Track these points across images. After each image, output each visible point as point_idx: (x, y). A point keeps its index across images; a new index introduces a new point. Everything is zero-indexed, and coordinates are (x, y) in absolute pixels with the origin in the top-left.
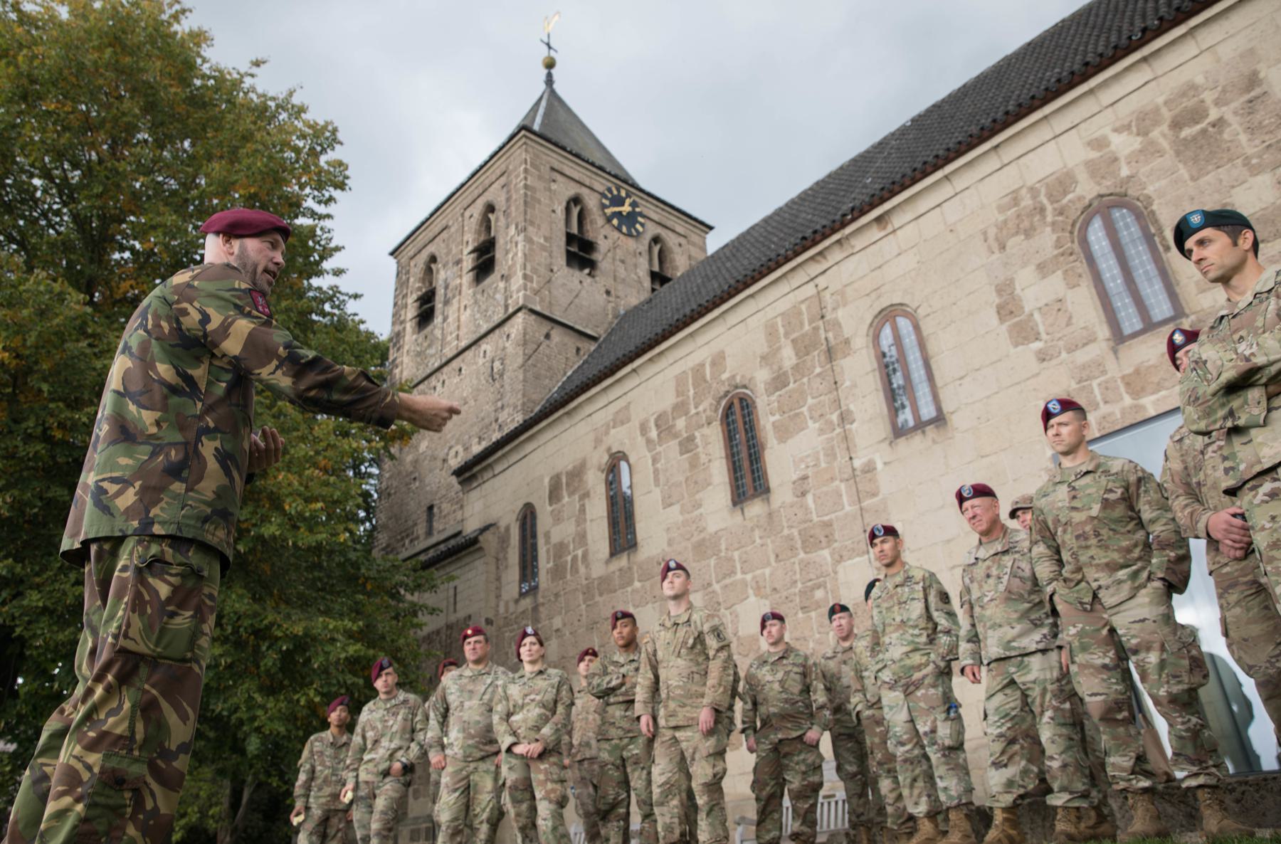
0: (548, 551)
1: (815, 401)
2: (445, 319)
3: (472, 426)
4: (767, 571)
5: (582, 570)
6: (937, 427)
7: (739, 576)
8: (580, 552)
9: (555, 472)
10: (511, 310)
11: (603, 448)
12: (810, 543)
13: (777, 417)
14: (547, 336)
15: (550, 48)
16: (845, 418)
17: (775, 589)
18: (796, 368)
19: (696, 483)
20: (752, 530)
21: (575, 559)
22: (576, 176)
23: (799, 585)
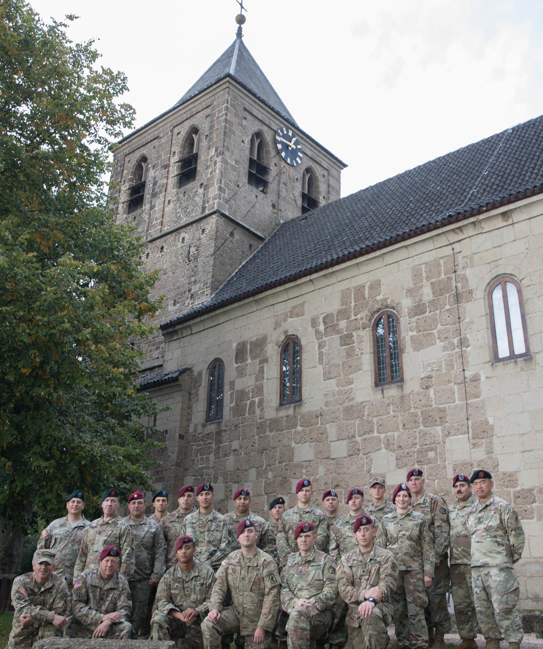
0: (232, 395)
1: (443, 327)
2: (152, 207)
3: (169, 291)
4: (396, 434)
5: (258, 412)
6: (525, 360)
7: (375, 434)
8: (257, 400)
9: (242, 340)
10: (207, 212)
11: (281, 330)
12: (428, 420)
13: (415, 333)
14: (232, 234)
15: (242, 7)
16: (463, 343)
17: (400, 447)
18: (432, 302)
19: (350, 367)
20: (388, 405)
21: (252, 403)
22: (260, 116)
23: (418, 447)
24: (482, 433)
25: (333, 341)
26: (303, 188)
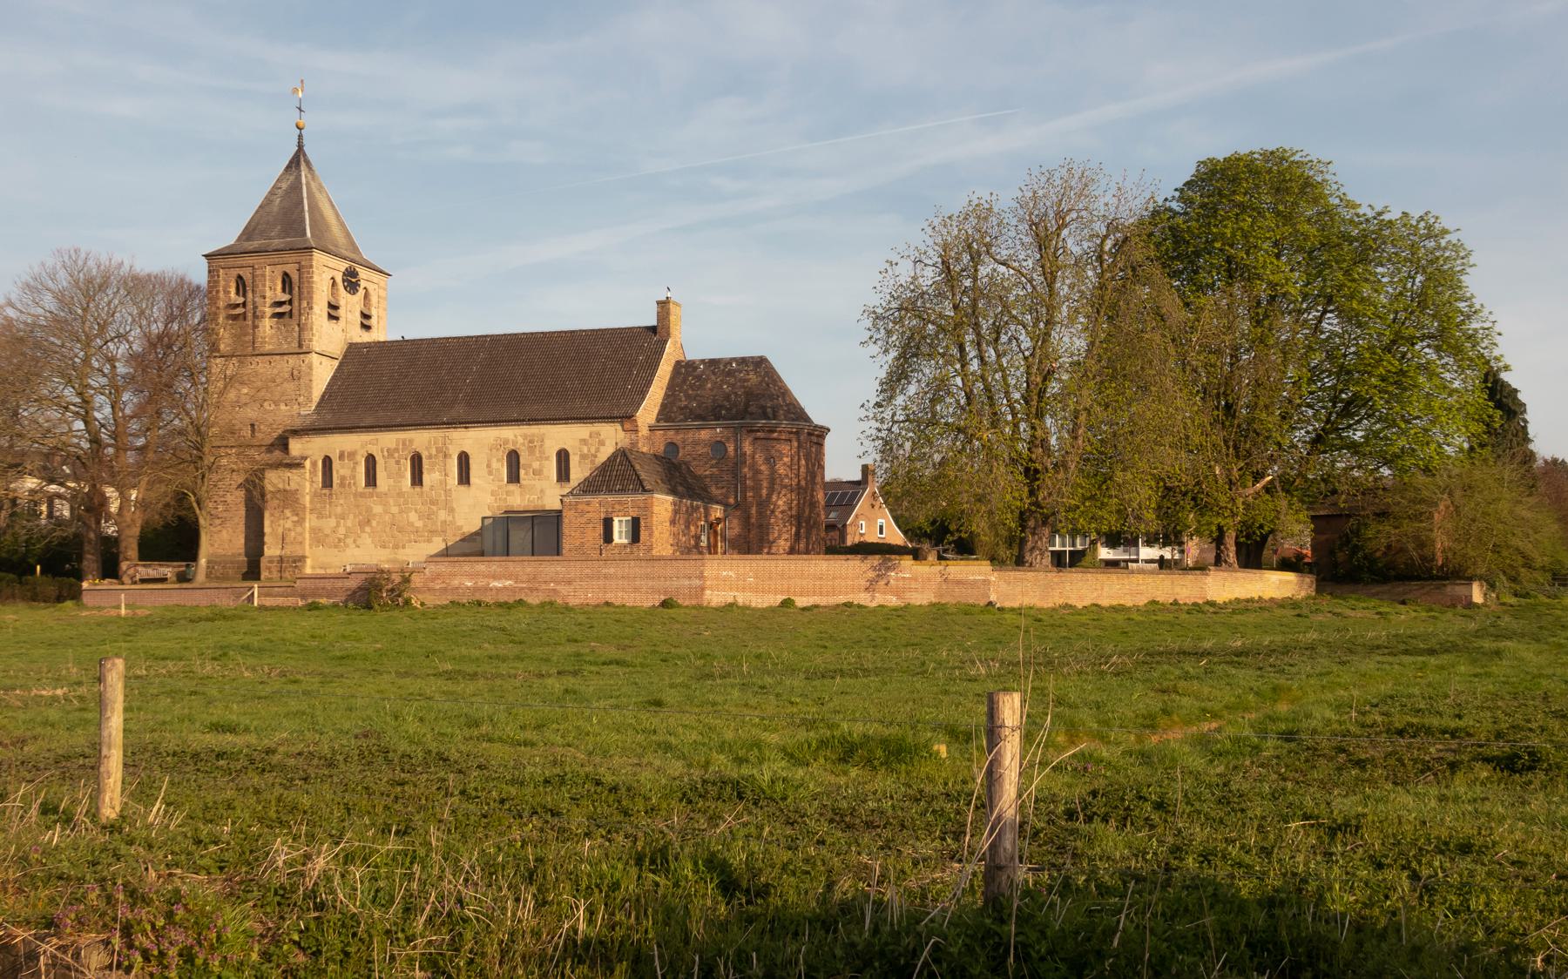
12: (432, 503)
24: (452, 511)
25: (392, 461)
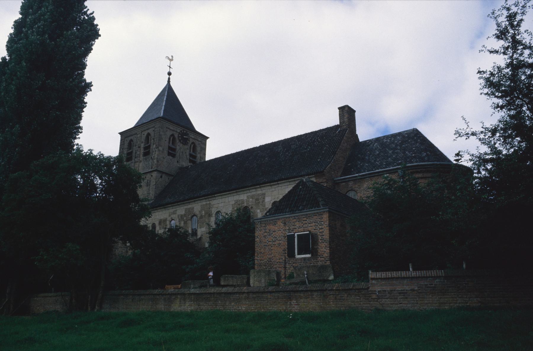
14: (161, 177)
22: (172, 128)
26: (190, 151)
